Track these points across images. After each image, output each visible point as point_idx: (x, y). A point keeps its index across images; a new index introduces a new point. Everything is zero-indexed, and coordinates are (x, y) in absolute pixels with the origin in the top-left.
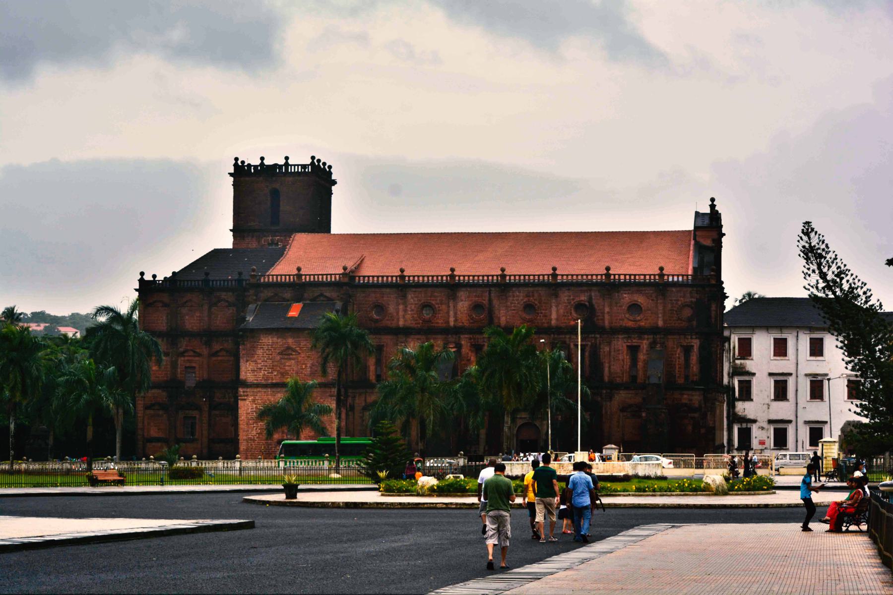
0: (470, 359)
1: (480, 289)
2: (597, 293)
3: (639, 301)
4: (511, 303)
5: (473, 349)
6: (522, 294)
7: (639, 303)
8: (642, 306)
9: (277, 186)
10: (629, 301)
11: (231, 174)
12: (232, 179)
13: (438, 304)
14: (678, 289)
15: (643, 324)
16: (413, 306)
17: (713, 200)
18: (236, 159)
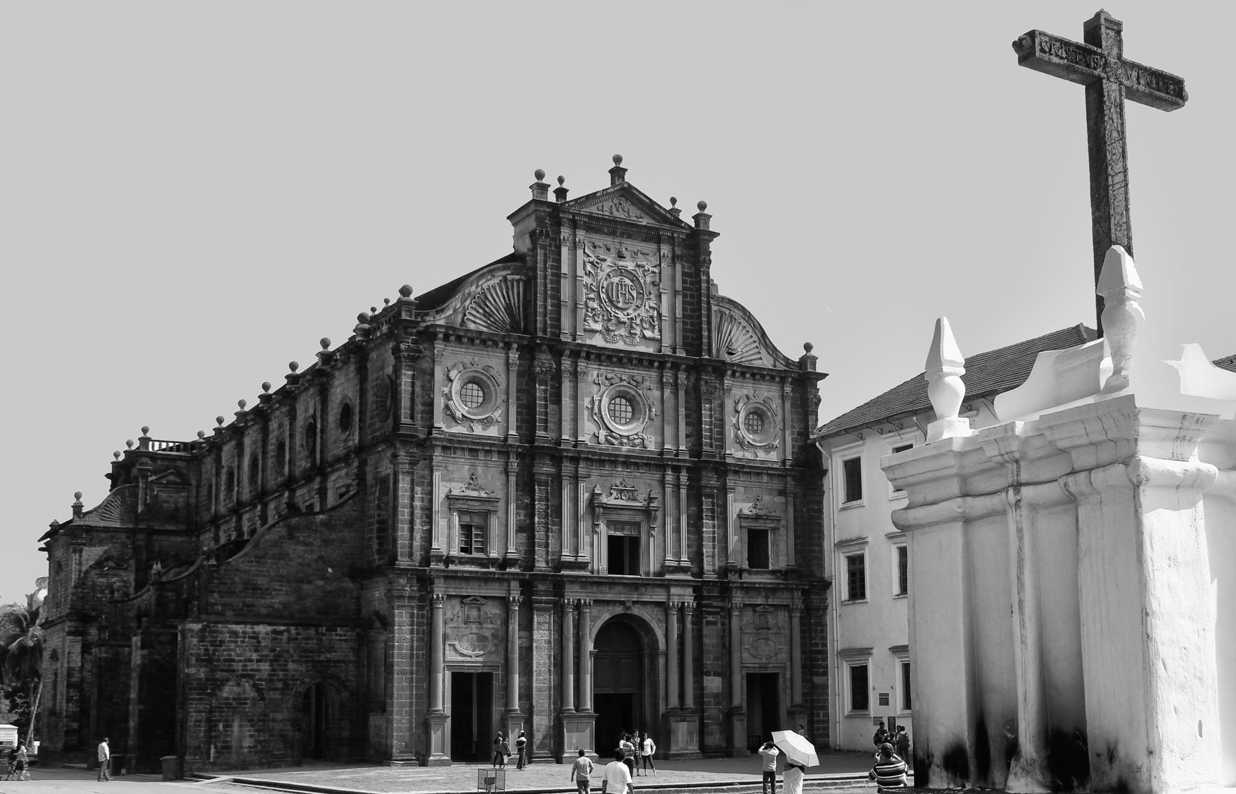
3: (350, 395)
7: (348, 402)
17: (618, 159)
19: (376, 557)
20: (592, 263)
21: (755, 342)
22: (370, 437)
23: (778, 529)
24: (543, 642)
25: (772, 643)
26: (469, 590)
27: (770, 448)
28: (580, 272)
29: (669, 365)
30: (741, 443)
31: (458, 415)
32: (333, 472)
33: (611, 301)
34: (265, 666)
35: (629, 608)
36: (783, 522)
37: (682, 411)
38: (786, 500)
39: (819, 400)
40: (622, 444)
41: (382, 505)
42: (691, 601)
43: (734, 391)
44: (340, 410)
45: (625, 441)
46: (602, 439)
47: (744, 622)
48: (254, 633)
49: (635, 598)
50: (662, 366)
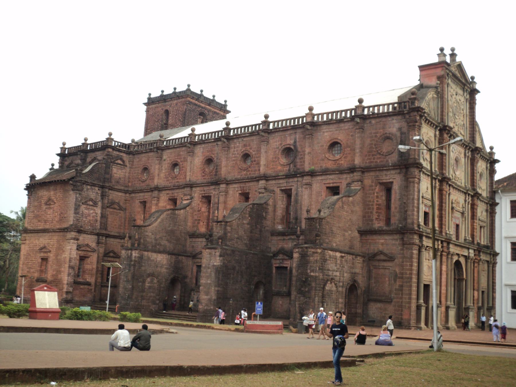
0: (201, 210)
1: (210, 144)
2: (302, 136)
3: (339, 138)
4: (233, 154)
5: (204, 200)
6: (241, 145)
8: (342, 143)
9: (168, 108)
10: (329, 139)
11: (145, 104)
12: (145, 107)
13: (181, 161)
14: (377, 120)
15: (342, 162)
16: (166, 166)
18: (150, 95)
19: (376, 222)
22: (368, 161)
28: (449, 99)
29: (468, 148)
32: (321, 175)
34: (338, 274)
35: (459, 257)
37: (469, 169)
38: (487, 215)
39: (496, 172)
41: (379, 197)
44: (329, 144)
46: (454, 177)
48: (335, 256)
50: (467, 146)
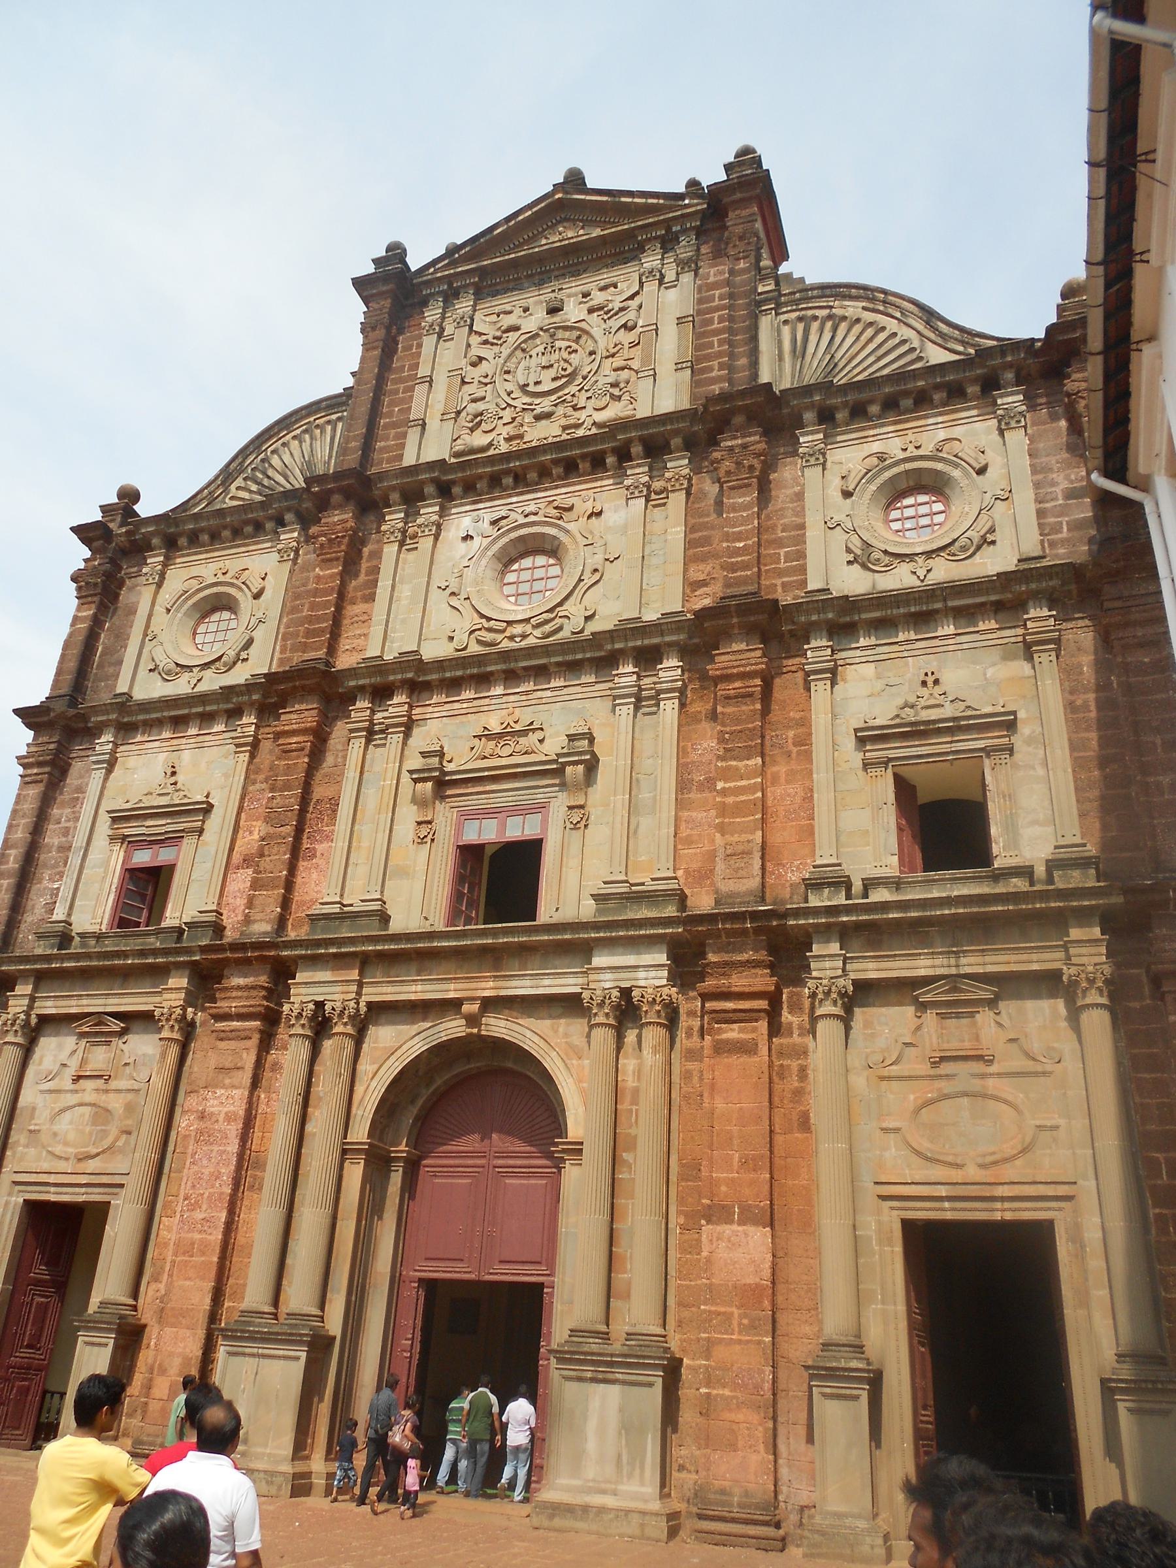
20: (486, 342)
21: (904, 342)
23: (1011, 750)
24: (221, 1119)
25: (1004, 1106)
26: (85, 1002)
27: (964, 549)
29: (636, 449)
30: (863, 559)
31: (163, 662)
33: (523, 388)
36: (1025, 730)
40: (512, 638)
42: (664, 982)
43: (834, 456)
45: (518, 629)
47: (881, 1043)
49: (488, 988)
50: (624, 455)
